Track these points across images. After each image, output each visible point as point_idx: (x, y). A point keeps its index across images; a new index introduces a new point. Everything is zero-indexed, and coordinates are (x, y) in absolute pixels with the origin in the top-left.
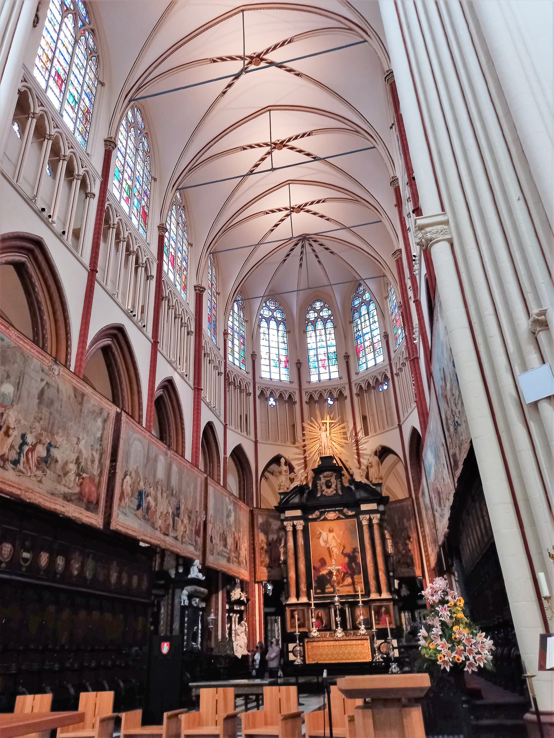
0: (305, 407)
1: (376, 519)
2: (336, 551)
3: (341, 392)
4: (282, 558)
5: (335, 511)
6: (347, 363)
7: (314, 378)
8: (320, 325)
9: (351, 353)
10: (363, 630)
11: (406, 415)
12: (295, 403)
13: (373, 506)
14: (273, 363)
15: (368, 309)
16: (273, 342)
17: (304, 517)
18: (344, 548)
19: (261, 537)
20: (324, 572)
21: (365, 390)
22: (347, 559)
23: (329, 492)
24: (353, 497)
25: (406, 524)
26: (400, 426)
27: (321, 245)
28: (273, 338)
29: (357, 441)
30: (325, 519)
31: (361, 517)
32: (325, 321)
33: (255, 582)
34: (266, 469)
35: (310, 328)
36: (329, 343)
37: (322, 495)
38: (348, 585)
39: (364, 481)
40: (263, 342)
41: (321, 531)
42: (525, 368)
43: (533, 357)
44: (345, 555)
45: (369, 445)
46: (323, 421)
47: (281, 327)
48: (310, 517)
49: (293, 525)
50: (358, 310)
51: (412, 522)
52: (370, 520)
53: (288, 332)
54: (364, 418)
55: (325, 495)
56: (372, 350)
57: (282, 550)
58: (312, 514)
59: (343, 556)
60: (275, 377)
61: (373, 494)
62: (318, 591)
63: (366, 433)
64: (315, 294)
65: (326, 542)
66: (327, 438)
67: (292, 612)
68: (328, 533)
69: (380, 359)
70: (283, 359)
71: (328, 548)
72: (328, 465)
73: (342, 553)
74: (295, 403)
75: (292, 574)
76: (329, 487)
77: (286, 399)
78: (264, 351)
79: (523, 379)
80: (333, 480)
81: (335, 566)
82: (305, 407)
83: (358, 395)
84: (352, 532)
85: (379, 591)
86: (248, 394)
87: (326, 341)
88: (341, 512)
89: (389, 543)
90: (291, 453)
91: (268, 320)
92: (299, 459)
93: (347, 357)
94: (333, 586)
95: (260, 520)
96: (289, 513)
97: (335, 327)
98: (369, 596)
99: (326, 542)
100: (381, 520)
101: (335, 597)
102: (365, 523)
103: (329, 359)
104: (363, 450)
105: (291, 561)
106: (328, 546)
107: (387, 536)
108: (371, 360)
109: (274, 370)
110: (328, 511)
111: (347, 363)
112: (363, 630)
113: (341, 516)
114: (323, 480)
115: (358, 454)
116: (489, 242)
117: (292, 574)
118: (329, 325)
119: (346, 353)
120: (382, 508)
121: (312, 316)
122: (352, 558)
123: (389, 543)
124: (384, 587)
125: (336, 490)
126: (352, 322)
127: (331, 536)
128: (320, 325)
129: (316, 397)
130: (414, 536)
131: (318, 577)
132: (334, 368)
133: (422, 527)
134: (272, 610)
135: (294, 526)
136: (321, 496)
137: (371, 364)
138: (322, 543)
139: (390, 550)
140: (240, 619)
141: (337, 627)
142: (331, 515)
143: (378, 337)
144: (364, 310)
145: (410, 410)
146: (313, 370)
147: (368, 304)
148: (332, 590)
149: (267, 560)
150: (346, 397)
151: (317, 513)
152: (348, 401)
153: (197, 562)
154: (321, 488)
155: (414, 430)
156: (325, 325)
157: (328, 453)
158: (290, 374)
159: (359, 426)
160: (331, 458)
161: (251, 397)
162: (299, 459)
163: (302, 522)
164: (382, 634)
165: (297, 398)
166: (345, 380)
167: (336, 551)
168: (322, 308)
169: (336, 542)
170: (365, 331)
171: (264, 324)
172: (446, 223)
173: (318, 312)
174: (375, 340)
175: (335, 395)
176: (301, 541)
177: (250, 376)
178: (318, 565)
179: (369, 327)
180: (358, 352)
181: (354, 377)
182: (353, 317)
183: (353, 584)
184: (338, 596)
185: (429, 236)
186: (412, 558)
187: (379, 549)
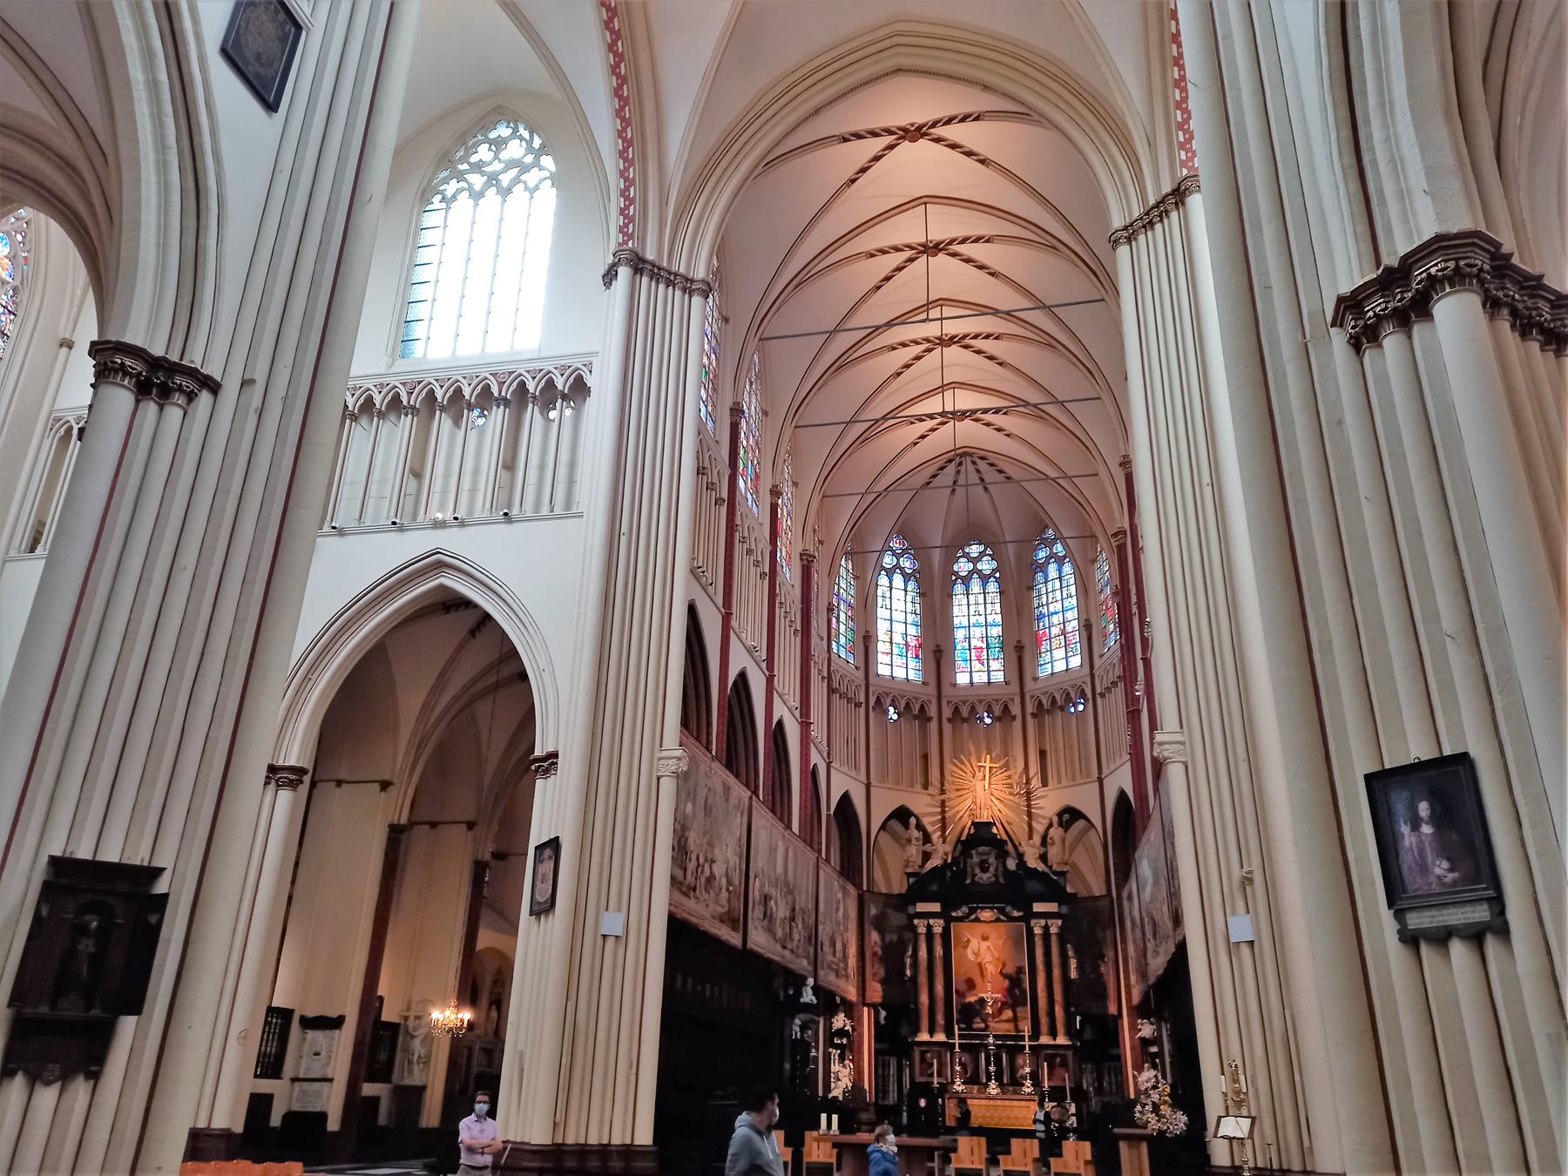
0: (947, 727)
1: (1055, 926)
2: (991, 969)
4: (908, 973)
6: (1020, 659)
7: (962, 679)
8: (976, 586)
9: (1026, 642)
10: (1028, 1087)
11: (1112, 767)
12: (929, 719)
13: (1052, 907)
14: (896, 651)
15: (1060, 570)
16: (897, 610)
17: (944, 915)
19: (875, 936)
20: (972, 999)
22: (1007, 983)
25: (1100, 935)
26: (1100, 781)
27: (992, 465)
28: (898, 605)
29: (1028, 793)
30: (977, 920)
31: (1033, 922)
32: (984, 579)
33: (865, 1004)
34: (883, 827)
35: (959, 588)
36: (990, 619)
39: (1041, 867)
40: (882, 613)
42: (1234, 913)
43: (1240, 904)
44: (1005, 976)
45: (1049, 803)
47: (911, 585)
50: (1043, 568)
51: (1109, 932)
52: (1046, 928)
53: (921, 595)
54: (1042, 754)
57: (908, 961)
60: (900, 673)
61: (1051, 886)
63: (1045, 783)
64: (971, 531)
65: (977, 954)
66: (984, 792)
67: (923, 1053)
69: (1075, 662)
70: (913, 643)
71: (980, 965)
72: (982, 835)
74: (929, 719)
75: (924, 998)
76: (985, 870)
77: (915, 712)
78: (882, 627)
80: (992, 860)
81: (990, 992)
82: (947, 727)
83: (1034, 715)
84: (1018, 943)
85: (1053, 1033)
86: (858, 705)
88: (1001, 911)
89: (1073, 964)
90: (923, 805)
91: (889, 573)
92: (933, 814)
93: (1019, 648)
94: (984, 1021)
95: (873, 911)
96: (922, 907)
99: (977, 954)
100: (1061, 928)
102: (1038, 931)
103: (988, 648)
105: (923, 979)
107: (1070, 953)
108: (1059, 659)
109: (898, 661)
111: (1020, 659)
112: (1028, 1087)
114: (976, 859)
115: (1029, 814)
117: (924, 998)
118: (992, 587)
120: (1065, 910)
121: (963, 567)
122: (1014, 981)
123: (1073, 964)
124: (1060, 1028)
125: (996, 876)
126: (1031, 588)
127: (984, 948)
128: (976, 586)
129: (965, 712)
130: (1110, 954)
132: (995, 665)
133: (1124, 941)
134: (883, 1046)
135: (929, 927)
137: (1060, 666)
138: (971, 957)
139: (1073, 975)
140: (842, 1058)
141: (989, 1079)
142: (986, 915)
143: (1075, 623)
144: (1052, 570)
145: (1118, 762)
146: (960, 663)
147: (1060, 562)
148: (982, 1025)
149: (882, 973)
150: (1014, 718)
151: (965, 909)
152: (1018, 724)
153: (811, 981)
155: (1122, 795)
156: (984, 586)
157: (985, 817)
158: (925, 670)
159: (1034, 768)
160: (989, 825)
161: (862, 710)
162: (933, 814)
163: (941, 922)
164: (1057, 1094)
165: (932, 711)
166: (1015, 688)
168: (982, 554)
170: (1052, 609)
171: (883, 580)
172: (1183, 743)
173: (975, 561)
174: (1069, 629)
175: (997, 711)
177: (861, 674)
178: (963, 987)
179: (1058, 600)
181: (1029, 685)
183: (1015, 1019)
185: (1166, 754)
187: (1056, 972)
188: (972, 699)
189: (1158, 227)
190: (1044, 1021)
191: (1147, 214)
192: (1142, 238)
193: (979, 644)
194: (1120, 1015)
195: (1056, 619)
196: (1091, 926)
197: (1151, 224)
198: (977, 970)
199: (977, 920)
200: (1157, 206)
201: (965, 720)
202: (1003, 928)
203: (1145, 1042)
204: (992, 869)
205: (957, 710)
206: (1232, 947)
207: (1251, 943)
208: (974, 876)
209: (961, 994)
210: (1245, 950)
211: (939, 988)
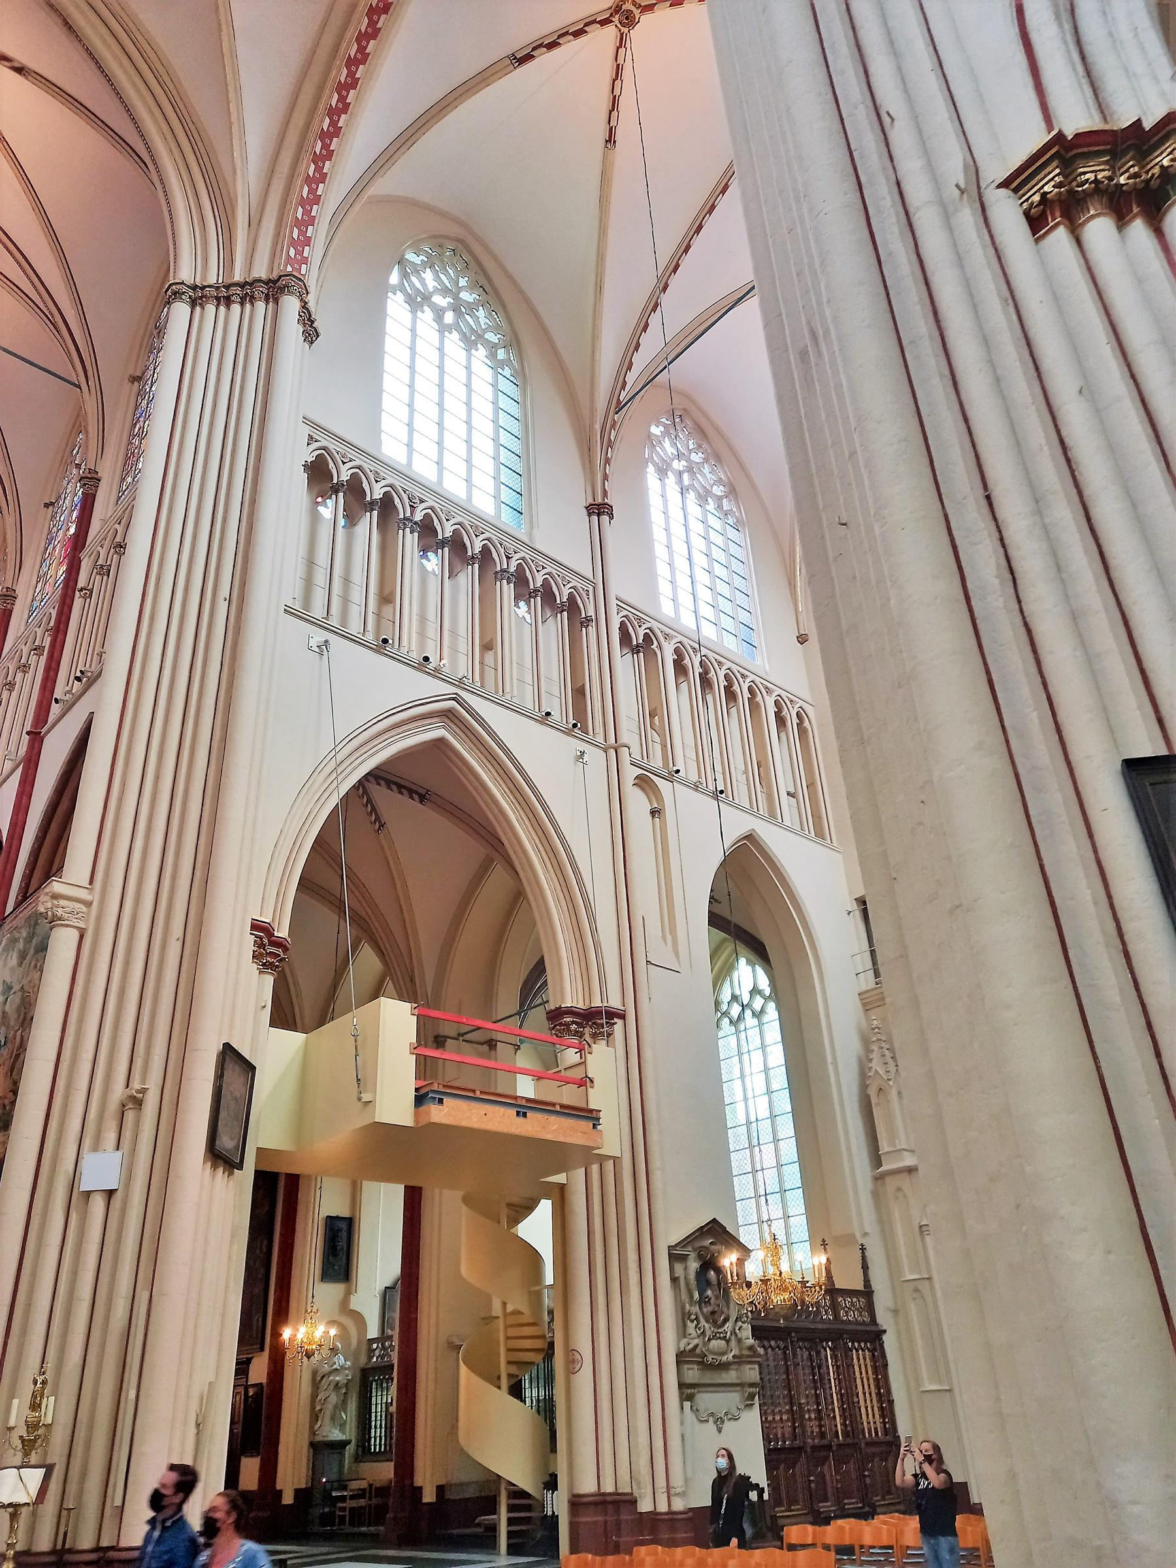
43: (111, 1136)
79: (88, 1159)
116: (127, 963)
172: (89, 904)
185: (60, 912)
189: (236, 308)
191: (227, 287)
192: (211, 308)
197: (228, 301)
200: (242, 285)
206: (77, 1197)
207: (110, 1193)
210: (98, 1203)
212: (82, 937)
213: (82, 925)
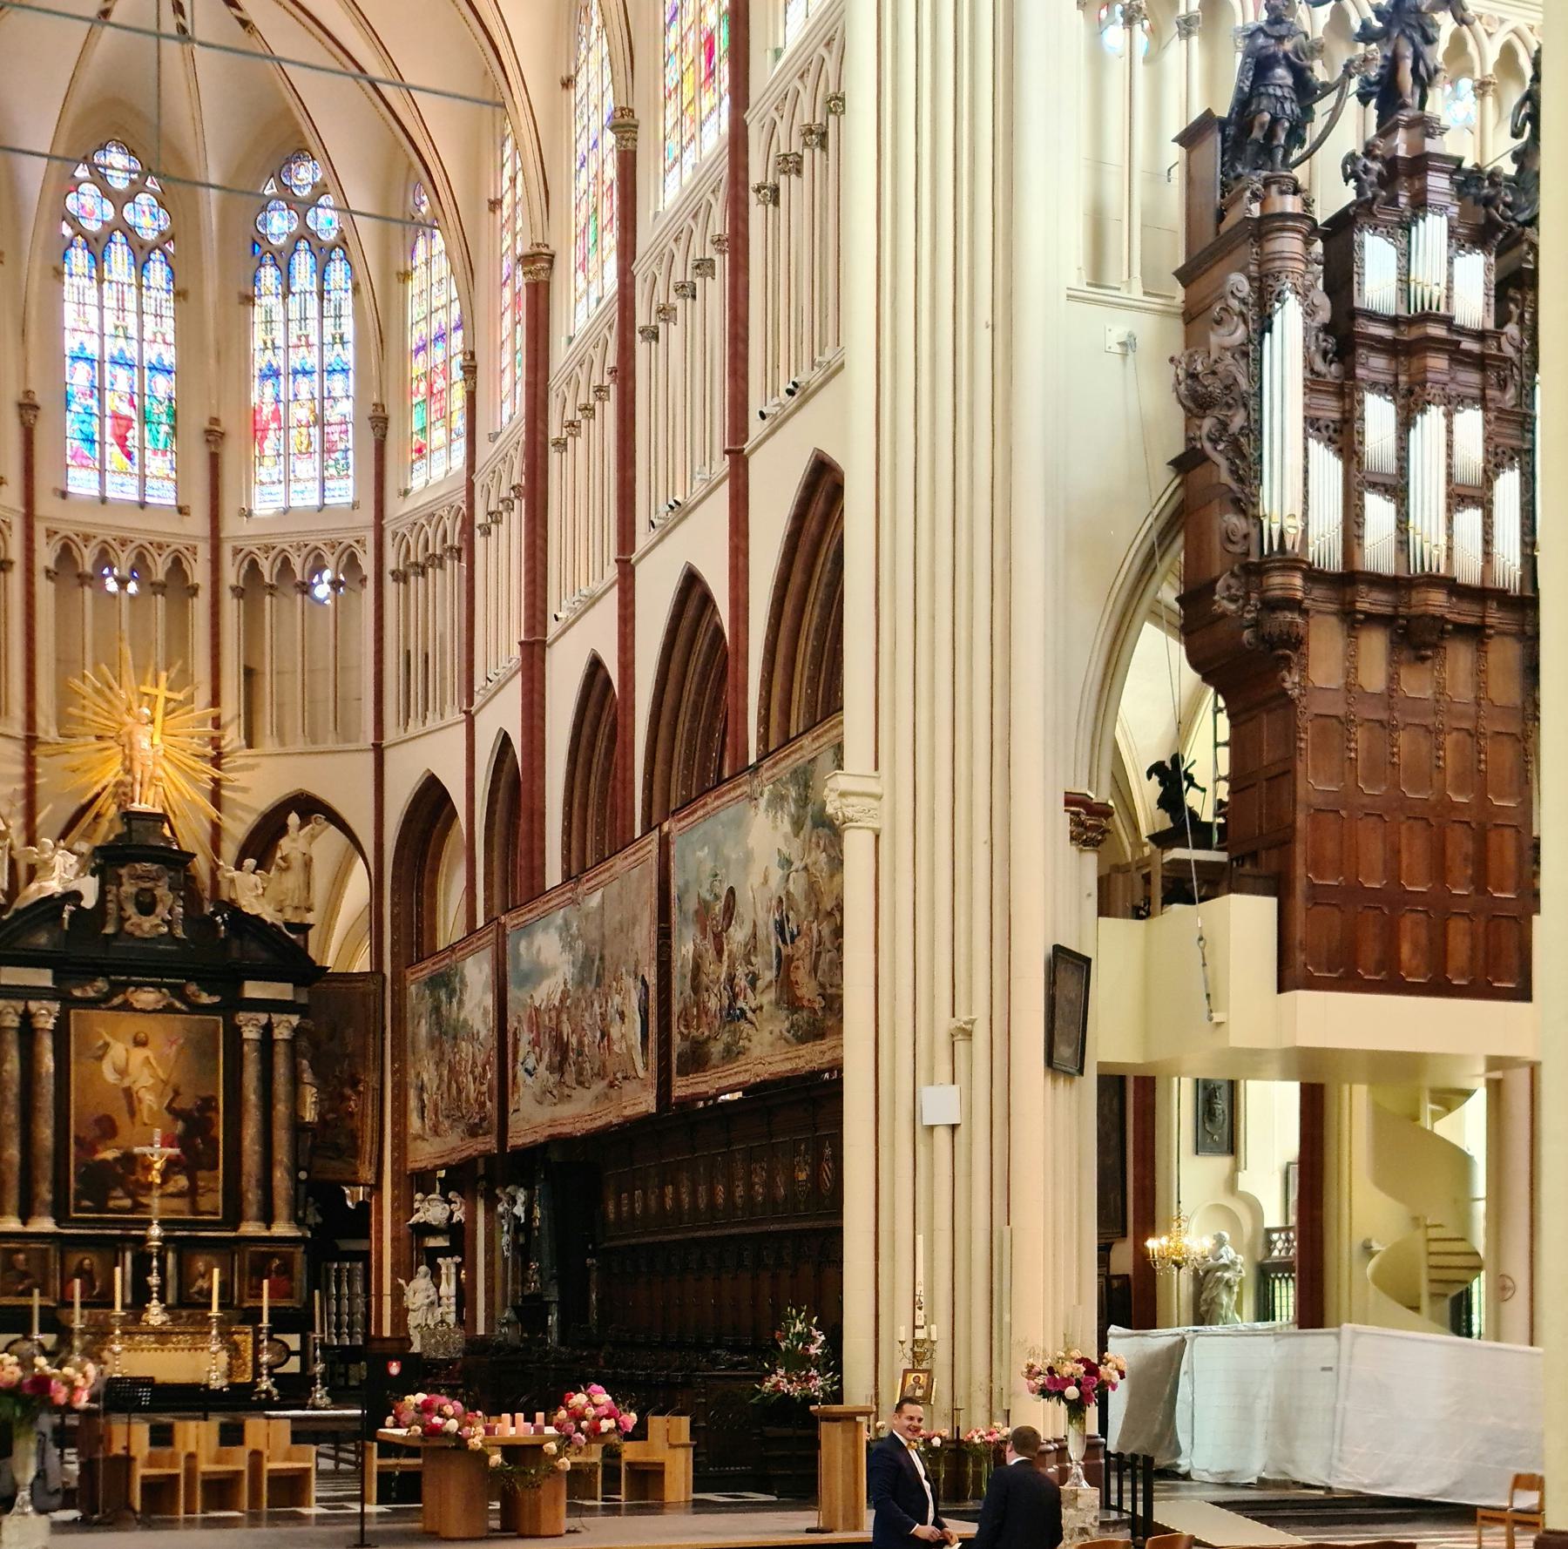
0: (45, 590)
2: (149, 1100)
3: (177, 562)
5: (158, 986)
18: (177, 1093)
21: (271, 586)
22: (180, 1126)
23: (146, 926)
24: (226, 955)
30: (126, 1006)
31: (242, 1017)
37: (120, 928)
38: (179, 1195)
41: (108, 1039)
43: (944, 1069)
46: (143, 689)
48: (77, 993)
49: (27, 1010)
52: (268, 1029)
55: (131, 934)
56: (316, 446)
58: (82, 987)
59: (168, 1117)
61: (284, 951)
62: (87, 1203)
65: (122, 1072)
68: (130, 1045)
71: (128, 1092)
73: (169, 1108)
76: (147, 908)
80: (162, 891)
82: (45, 590)
87: (141, 340)
88: (177, 991)
93: (214, 436)
94: (130, 1194)
97: (180, 295)
98: (236, 1230)
99: (122, 1072)
100: (297, 1031)
101: (149, 1223)
102: (251, 1033)
103: (145, 420)
104: (234, 789)
106: (126, 1083)
110: (139, 986)
113: (178, 1004)
119: (215, 421)
125: (169, 923)
126: (248, 300)
127: (136, 1059)
131: (88, 1166)
132: (159, 465)
136: (115, 936)
138: (110, 1076)
146: (73, 444)
148: (127, 1203)
151: (101, 984)
154: (122, 909)
163: (56, 1007)
167: (149, 1100)
169: (154, 1076)
175: (160, 571)
176: (48, 1062)
178: (92, 1133)
180: (257, 432)
182: (255, 279)
183: (192, 1193)
184: (162, 1223)
186: (353, 1136)
188: (103, 535)
190: (252, 1196)
193: (126, 410)
194: (377, 1187)
195: (305, 386)
196: (344, 1027)
198: (123, 1103)
199: (126, 1006)
201: (83, 579)
202: (177, 1023)
203: (426, 1229)
204: (161, 910)
205: (66, 554)
208: (122, 920)
209: (87, 1147)
211: (46, 1133)
212: (877, 837)
213: (876, 826)
